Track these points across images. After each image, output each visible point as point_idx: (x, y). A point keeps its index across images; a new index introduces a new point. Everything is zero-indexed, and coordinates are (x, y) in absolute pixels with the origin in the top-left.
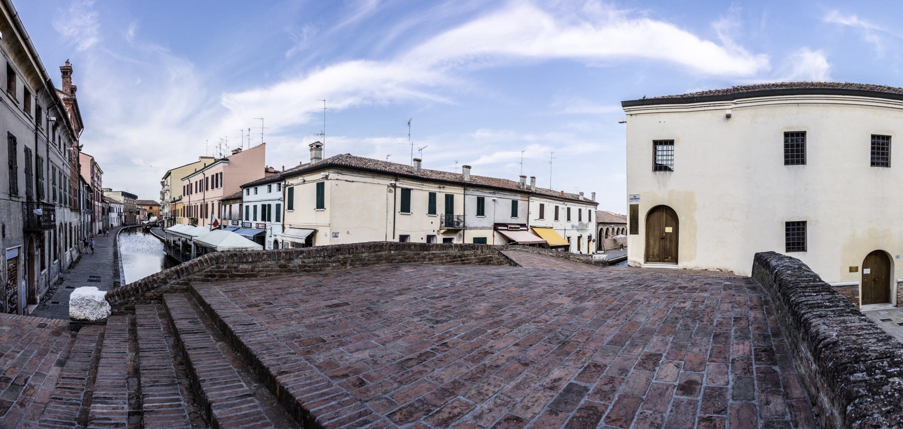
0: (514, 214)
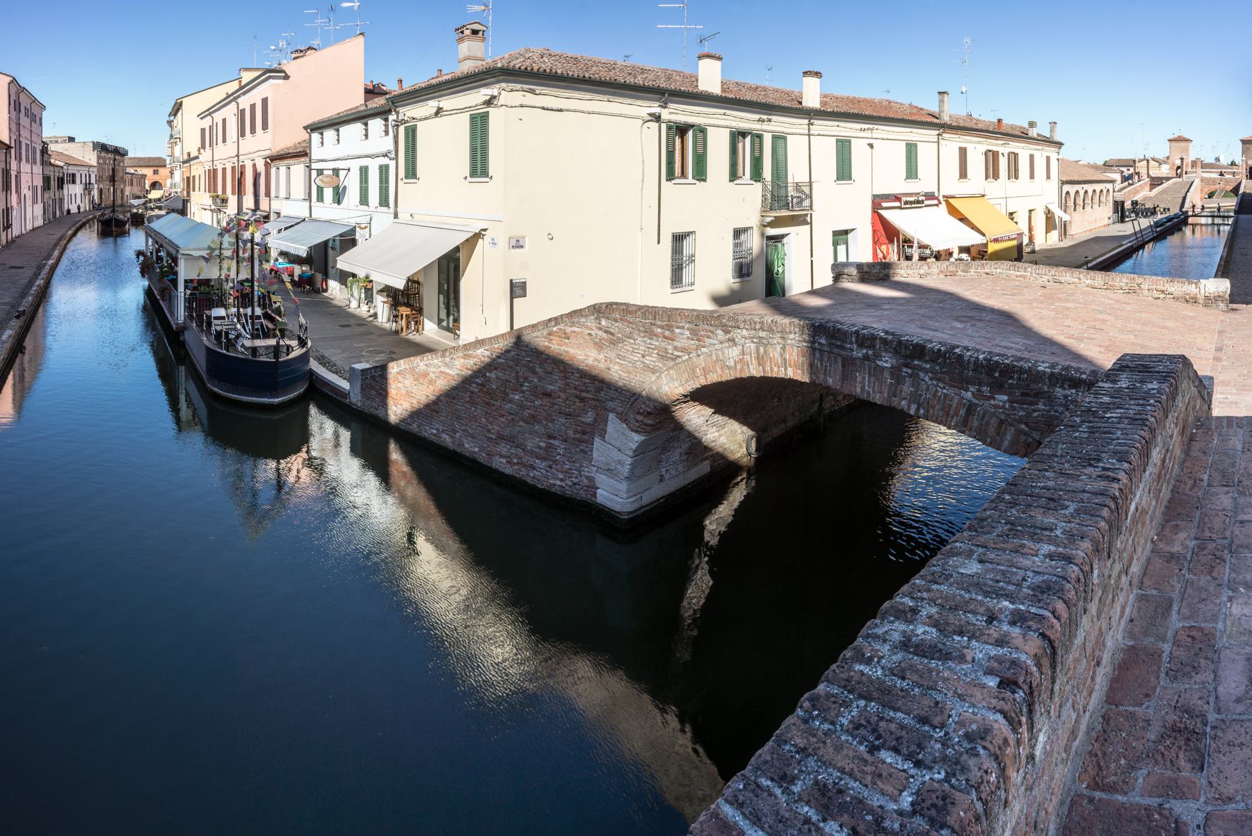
0: (912, 173)
